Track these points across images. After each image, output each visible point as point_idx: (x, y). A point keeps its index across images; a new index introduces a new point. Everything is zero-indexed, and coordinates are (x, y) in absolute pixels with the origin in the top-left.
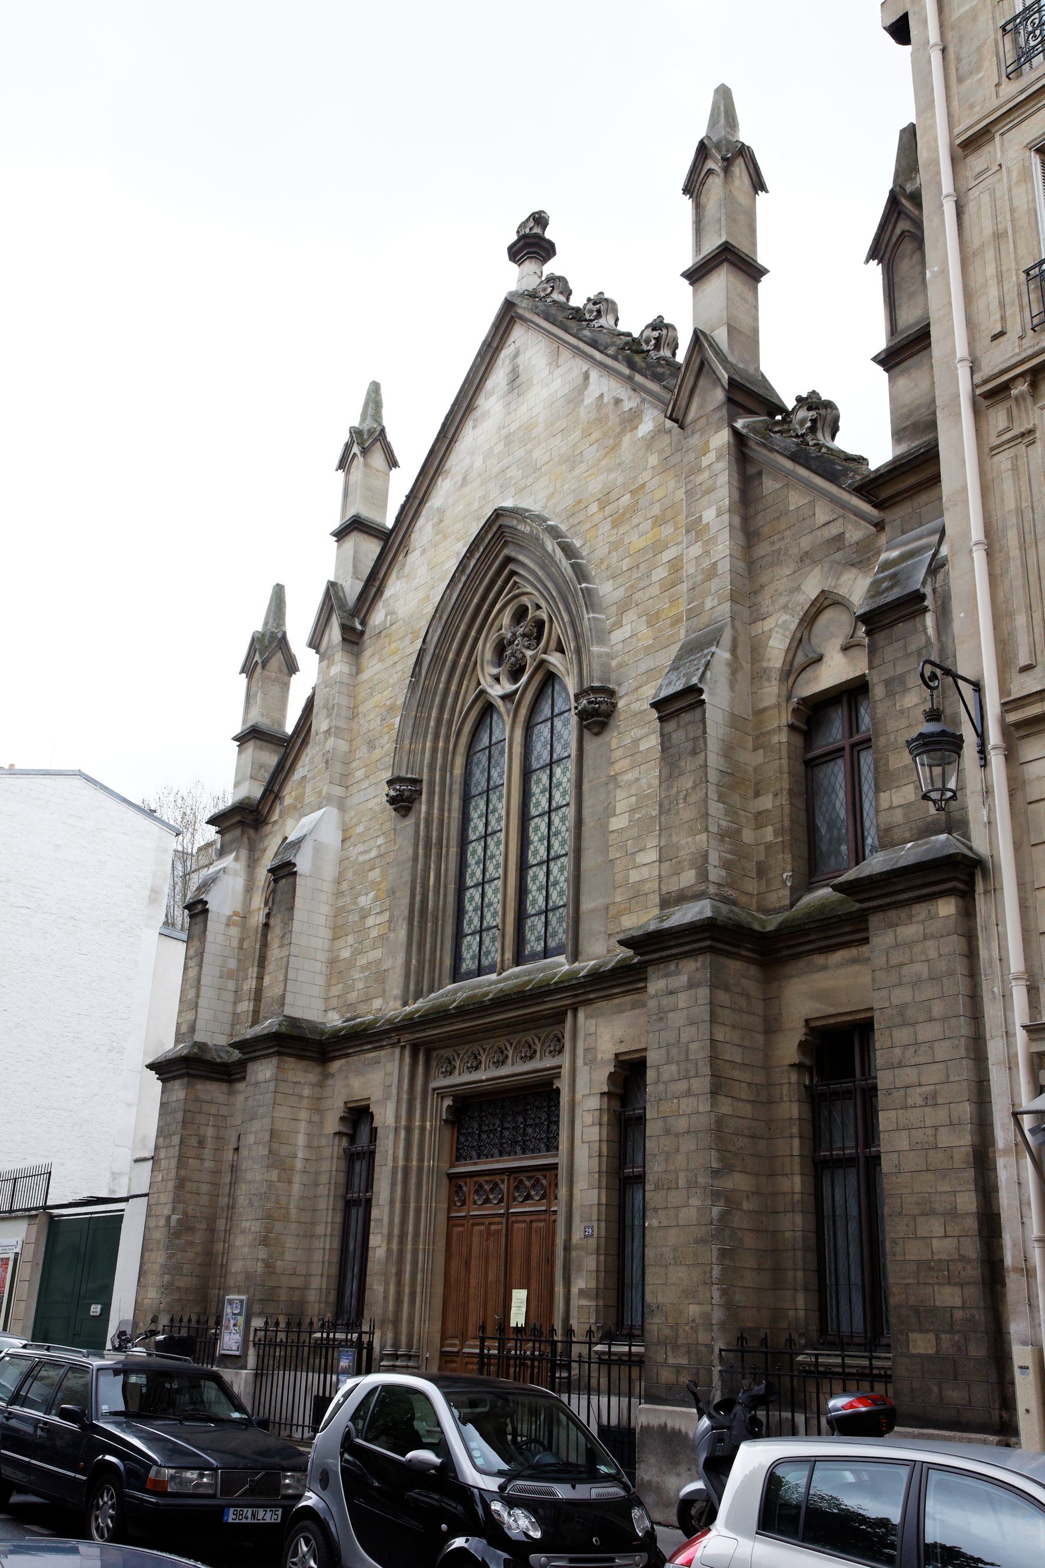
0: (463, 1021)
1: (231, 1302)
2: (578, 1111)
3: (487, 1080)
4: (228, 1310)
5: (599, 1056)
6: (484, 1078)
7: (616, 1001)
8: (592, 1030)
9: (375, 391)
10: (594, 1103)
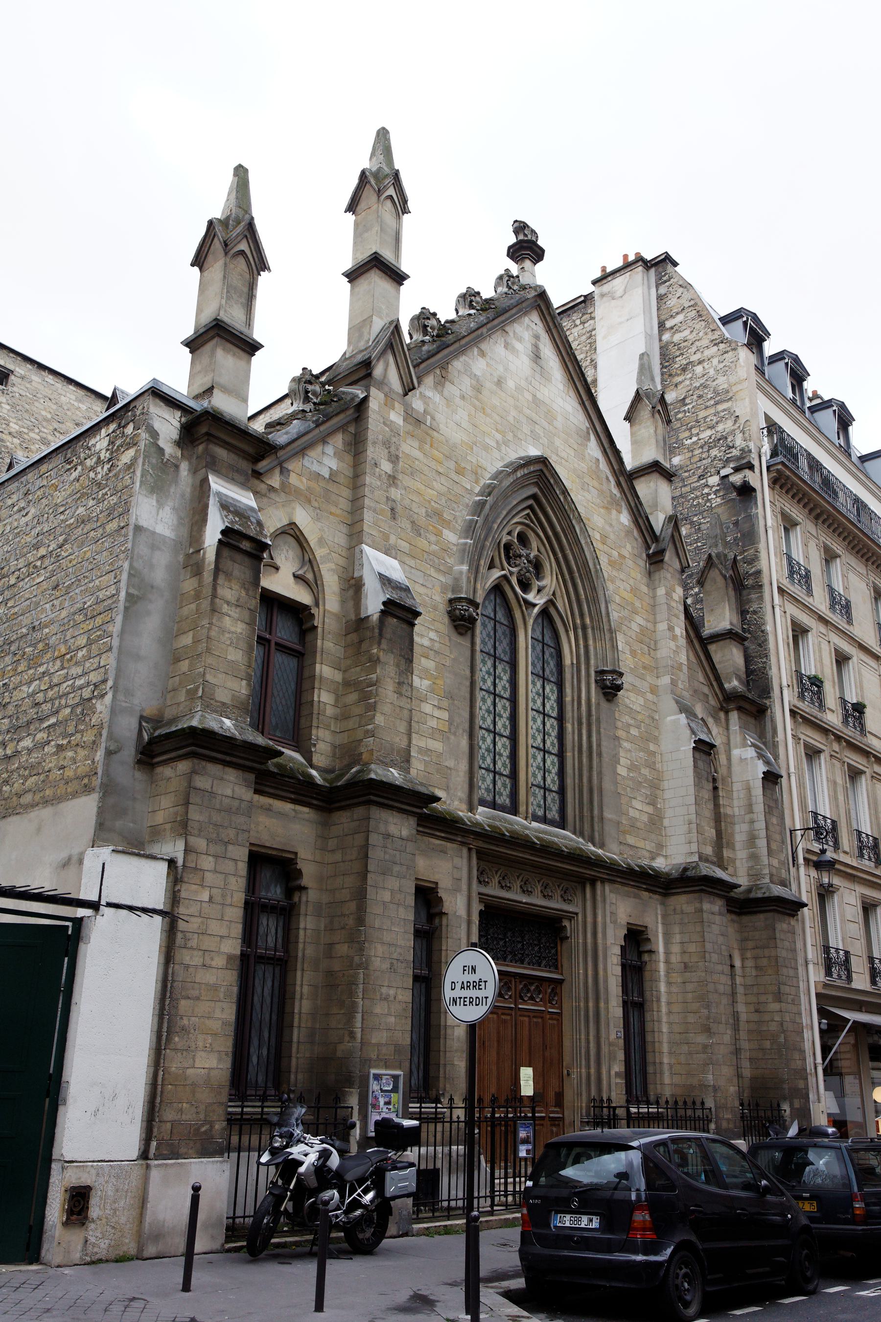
0: (532, 855)
1: (377, 1077)
2: (609, 953)
3: (526, 903)
4: (374, 1086)
5: (619, 920)
6: (524, 901)
7: (626, 888)
8: (614, 901)
9: (383, 136)
10: (617, 950)
